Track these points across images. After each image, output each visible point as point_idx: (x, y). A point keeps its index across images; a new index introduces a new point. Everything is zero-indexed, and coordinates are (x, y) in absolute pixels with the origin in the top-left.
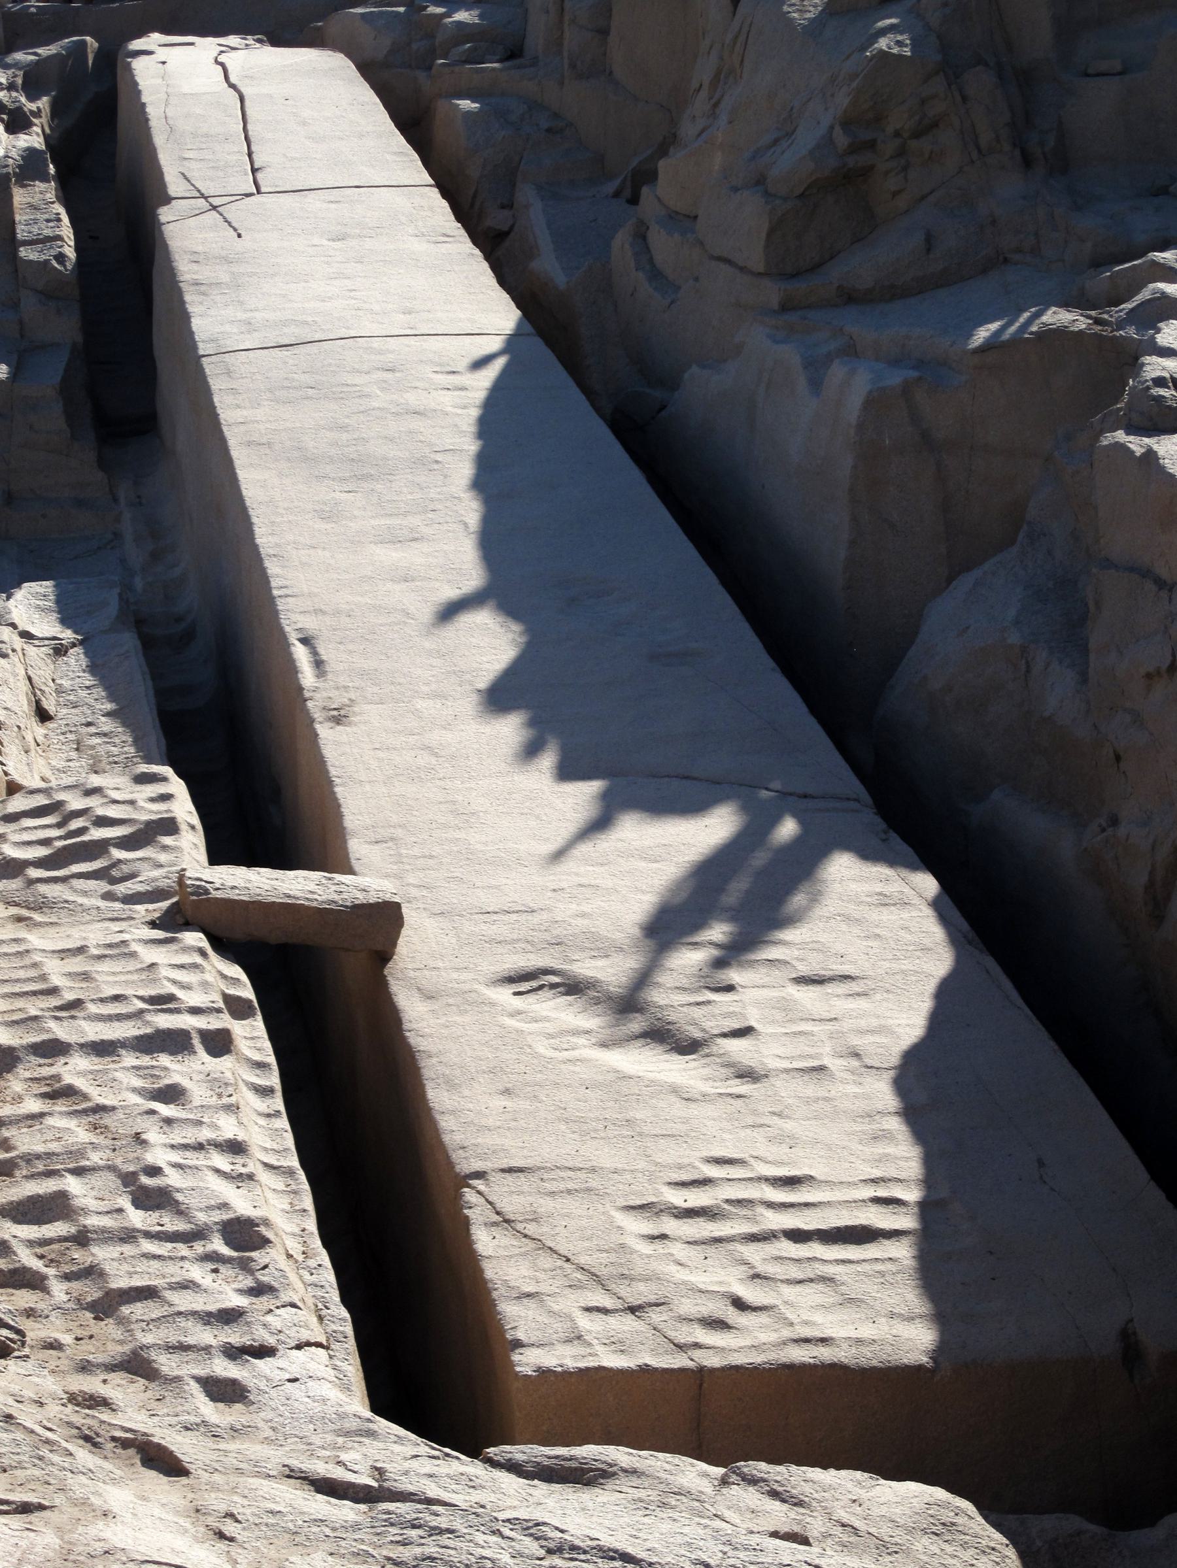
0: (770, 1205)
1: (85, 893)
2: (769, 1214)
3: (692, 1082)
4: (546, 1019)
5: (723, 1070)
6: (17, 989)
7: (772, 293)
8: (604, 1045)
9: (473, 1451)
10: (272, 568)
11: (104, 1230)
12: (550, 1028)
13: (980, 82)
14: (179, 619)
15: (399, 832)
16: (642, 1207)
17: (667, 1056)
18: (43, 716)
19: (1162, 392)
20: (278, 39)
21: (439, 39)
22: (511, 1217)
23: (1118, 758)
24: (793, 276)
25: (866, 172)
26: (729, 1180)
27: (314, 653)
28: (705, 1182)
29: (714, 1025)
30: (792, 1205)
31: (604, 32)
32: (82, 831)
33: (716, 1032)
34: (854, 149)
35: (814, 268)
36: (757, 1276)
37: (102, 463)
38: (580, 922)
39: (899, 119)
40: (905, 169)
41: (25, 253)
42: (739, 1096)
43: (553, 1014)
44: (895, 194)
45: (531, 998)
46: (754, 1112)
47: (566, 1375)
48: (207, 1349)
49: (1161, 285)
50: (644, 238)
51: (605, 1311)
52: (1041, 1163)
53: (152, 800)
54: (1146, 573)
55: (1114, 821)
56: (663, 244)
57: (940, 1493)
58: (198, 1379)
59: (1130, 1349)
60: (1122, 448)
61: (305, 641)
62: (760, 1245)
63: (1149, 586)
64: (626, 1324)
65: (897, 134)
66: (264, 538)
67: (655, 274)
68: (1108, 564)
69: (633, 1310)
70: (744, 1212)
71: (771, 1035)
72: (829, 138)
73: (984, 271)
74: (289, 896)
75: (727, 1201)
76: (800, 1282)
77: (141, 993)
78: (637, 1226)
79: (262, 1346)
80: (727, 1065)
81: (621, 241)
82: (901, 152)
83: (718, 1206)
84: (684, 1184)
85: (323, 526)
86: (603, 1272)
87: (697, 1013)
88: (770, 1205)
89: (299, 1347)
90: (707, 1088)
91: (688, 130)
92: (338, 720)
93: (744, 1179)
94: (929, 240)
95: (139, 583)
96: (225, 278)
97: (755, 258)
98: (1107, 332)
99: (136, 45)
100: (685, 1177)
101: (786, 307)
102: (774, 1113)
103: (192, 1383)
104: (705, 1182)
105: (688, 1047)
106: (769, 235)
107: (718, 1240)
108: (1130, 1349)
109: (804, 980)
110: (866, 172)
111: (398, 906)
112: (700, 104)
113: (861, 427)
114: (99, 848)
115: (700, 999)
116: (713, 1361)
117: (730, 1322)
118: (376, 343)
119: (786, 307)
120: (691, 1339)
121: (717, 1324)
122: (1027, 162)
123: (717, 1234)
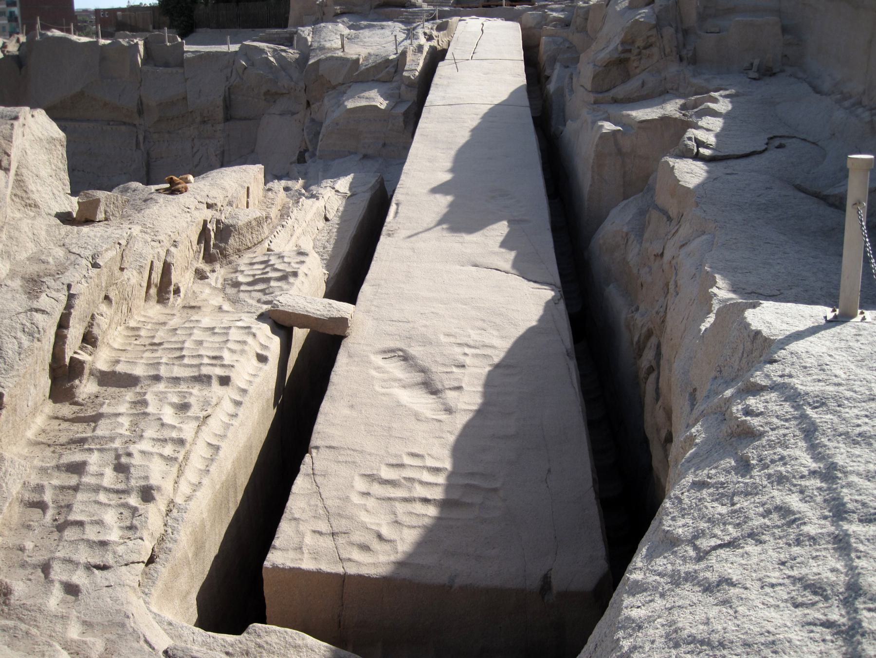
0: (422, 483)
1: (253, 298)
2: (418, 487)
3: (425, 411)
4: (388, 372)
5: (441, 406)
6: (173, 346)
7: (591, 97)
8: (404, 387)
10: (403, 177)
11: (89, 485)
12: (386, 376)
13: (668, 32)
15: (383, 282)
16: (369, 476)
17: (425, 395)
18: (327, 219)
19: (689, 142)
20: (507, 20)
21: (548, 20)
22: (316, 472)
24: (601, 93)
25: (627, 60)
27: (397, 209)
28: (401, 466)
29: (448, 383)
30: (430, 484)
31: (586, 19)
32: (267, 272)
33: (447, 387)
34: (625, 51)
35: (607, 91)
36: (396, 522)
38: (423, 329)
39: (640, 43)
40: (641, 59)
41: (405, 74)
42: (440, 421)
43: (391, 370)
44: (636, 68)
45: (388, 361)
46: (442, 431)
47: (284, 569)
48: (77, 564)
49: (709, 104)
51: (320, 533)
52: (549, 471)
53: (297, 263)
54: (665, 212)
58: (61, 583)
59: (546, 583)
61: (397, 204)
63: (665, 219)
64: (327, 543)
65: (639, 48)
68: (656, 207)
69: (333, 534)
70: (409, 484)
72: (616, 48)
73: (660, 95)
75: (405, 478)
76: (415, 527)
77: (208, 354)
78: (361, 485)
79: (104, 565)
80: (444, 404)
82: (640, 53)
83: (399, 480)
84: (392, 465)
85: (428, 164)
86: (332, 510)
87: (445, 376)
88: (422, 483)
89: (126, 565)
90: (430, 414)
92: (389, 235)
94: (643, 84)
96: (445, 83)
97: (589, 86)
98: (685, 119)
100: (395, 462)
101: (595, 103)
102: (448, 432)
103: (57, 585)
104: (401, 466)
105: (435, 392)
106: (594, 78)
107: (390, 499)
108: (546, 583)
110: (627, 60)
111: (347, 319)
113: (597, 145)
114: (268, 280)
115: (449, 370)
116: (352, 570)
117: (371, 547)
118: (477, 106)
119: (595, 103)
120: (348, 556)
121: (365, 548)
122: (681, 59)
123: (392, 495)
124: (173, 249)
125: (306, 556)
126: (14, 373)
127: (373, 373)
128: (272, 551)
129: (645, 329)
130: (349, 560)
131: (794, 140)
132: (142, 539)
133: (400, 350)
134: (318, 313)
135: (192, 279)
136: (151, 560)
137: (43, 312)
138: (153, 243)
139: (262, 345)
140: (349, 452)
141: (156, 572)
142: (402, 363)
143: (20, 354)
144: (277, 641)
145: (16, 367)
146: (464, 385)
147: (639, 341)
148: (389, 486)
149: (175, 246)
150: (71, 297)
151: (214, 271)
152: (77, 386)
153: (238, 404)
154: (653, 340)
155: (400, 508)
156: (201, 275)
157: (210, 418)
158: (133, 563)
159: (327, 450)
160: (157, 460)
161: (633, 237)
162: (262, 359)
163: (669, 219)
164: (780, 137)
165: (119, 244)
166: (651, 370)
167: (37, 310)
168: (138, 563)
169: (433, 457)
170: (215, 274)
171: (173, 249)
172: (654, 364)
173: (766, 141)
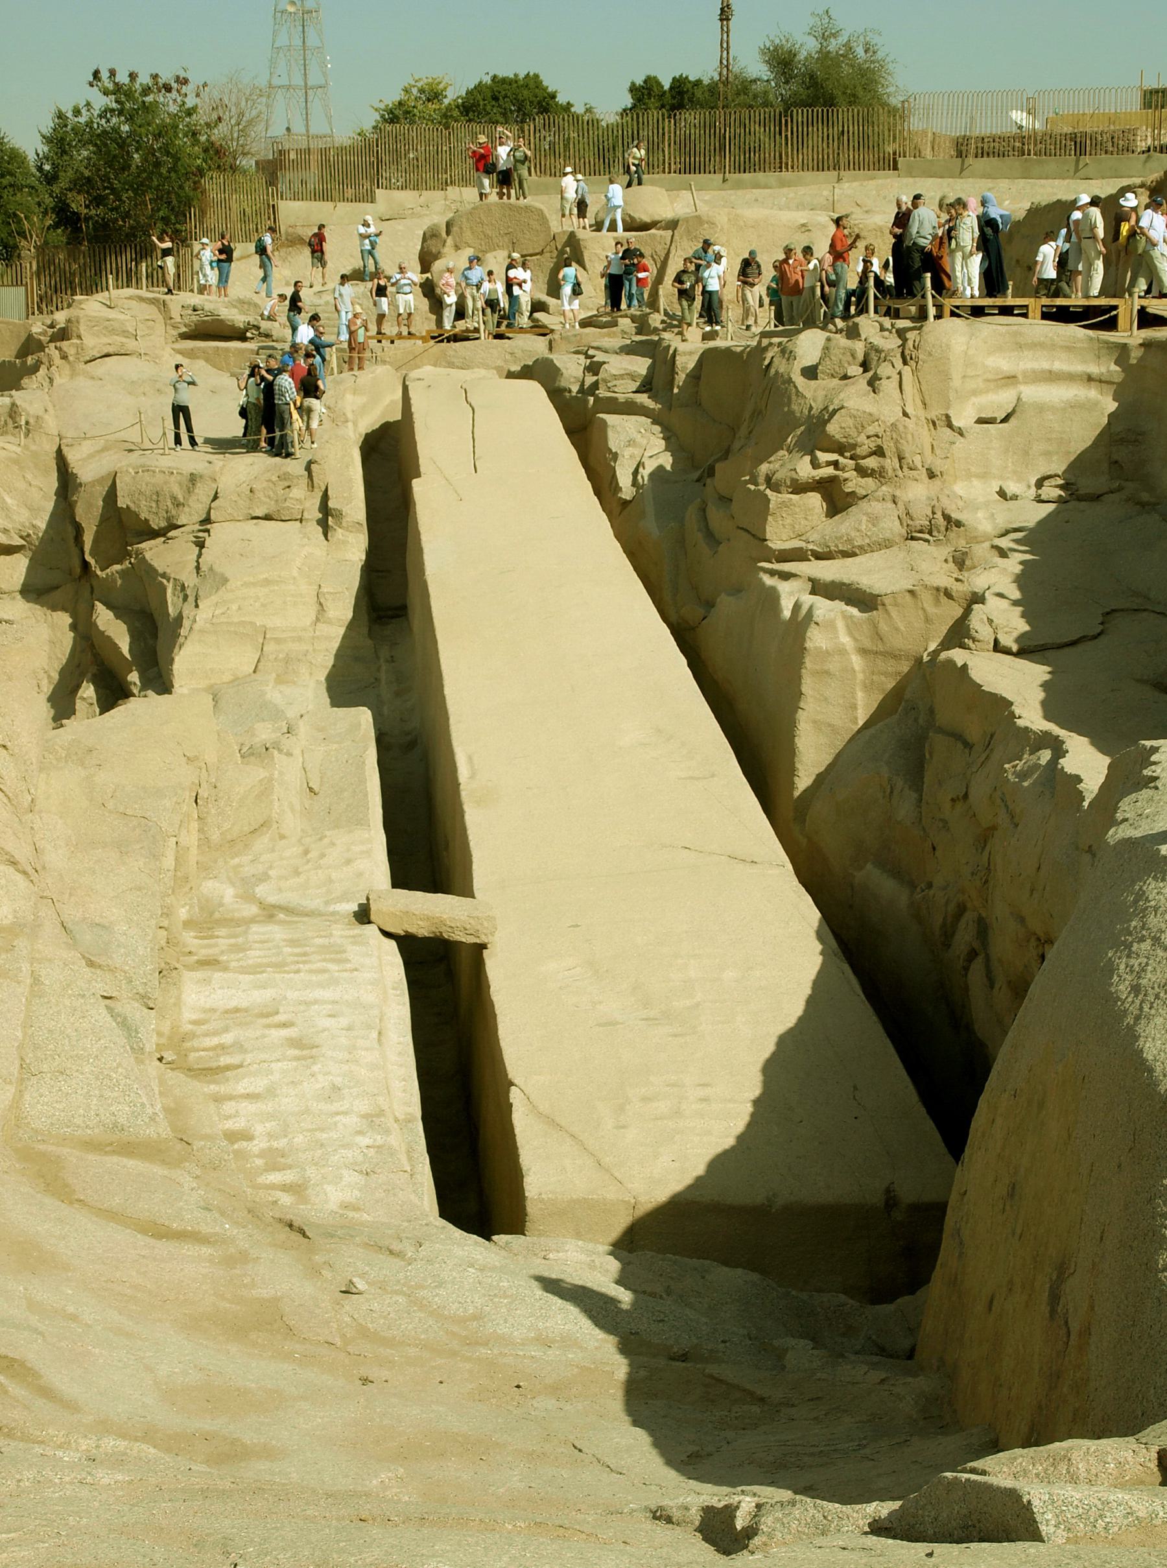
9: (488, 1239)
14: (408, 734)
23: (934, 849)
37: (370, 634)
50: (704, 510)
52: (855, 1088)
54: (959, 737)
55: (930, 885)
56: (716, 517)
57: (755, 1277)
59: (891, 1201)
60: (951, 662)
63: (960, 745)
66: (447, 691)
67: (710, 535)
68: (941, 730)
81: (691, 514)
91: (737, 445)
95: (386, 710)
99: (413, 374)
108: (891, 1201)
112: (743, 431)
129: (952, 907)
131: (1145, 614)
147: (944, 925)
154: (969, 916)
161: (900, 783)
163: (968, 745)
164: (1122, 610)
166: (973, 954)
172: (976, 945)
173: (1100, 619)
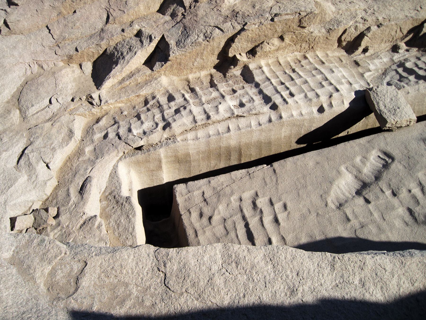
2: (257, 218)
8: (356, 177)
26: (274, 209)
33: (366, 196)
62: (242, 218)
71: (368, 208)
74: (378, 103)
75: (261, 210)
80: (346, 201)
83: (258, 208)
89: (126, 143)
93: (275, 211)
100: (274, 200)
109: (410, 211)
111: (387, 122)
123: (245, 211)
124: (374, 28)
125: (186, 197)
126: (183, 50)
127: (358, 159)
128: (185, 184)
130: (190, 213)
132: (142, 139)
133: (393, 159)
134: (382, 108)
135: (388, 48)
136: (139, 148)
137: (222, 30)
138: (360, 20)
139: (331, 103)
140: (275, 180)
141: (137, 154)
142: (381, 166)
143: (192, 43)
144: (127, 208)
145: (186, 48)
146: (373, 203)
148: (252, 206)
149: (378, 26)
150: (243, 30)
151: (407, 51)
152: (231, 68)
153: (270, 121)
155: (238, 218)
156: (395, 49)
157: (242, 118)
158: (128, 144)
159: (272, 170)
160: (191, 118)
162: (321, 110)
165: (300, 14)
167: (219, 28)
168: (130, 146)
169: (288, 215)
170: (406, 53)
171: (374, 28)
